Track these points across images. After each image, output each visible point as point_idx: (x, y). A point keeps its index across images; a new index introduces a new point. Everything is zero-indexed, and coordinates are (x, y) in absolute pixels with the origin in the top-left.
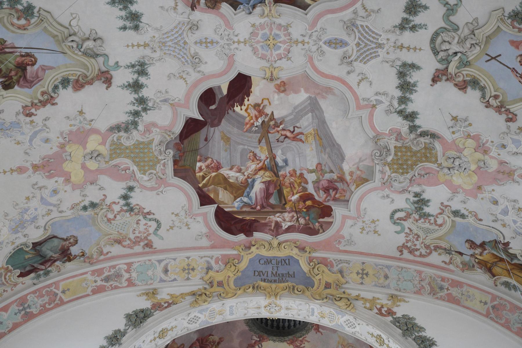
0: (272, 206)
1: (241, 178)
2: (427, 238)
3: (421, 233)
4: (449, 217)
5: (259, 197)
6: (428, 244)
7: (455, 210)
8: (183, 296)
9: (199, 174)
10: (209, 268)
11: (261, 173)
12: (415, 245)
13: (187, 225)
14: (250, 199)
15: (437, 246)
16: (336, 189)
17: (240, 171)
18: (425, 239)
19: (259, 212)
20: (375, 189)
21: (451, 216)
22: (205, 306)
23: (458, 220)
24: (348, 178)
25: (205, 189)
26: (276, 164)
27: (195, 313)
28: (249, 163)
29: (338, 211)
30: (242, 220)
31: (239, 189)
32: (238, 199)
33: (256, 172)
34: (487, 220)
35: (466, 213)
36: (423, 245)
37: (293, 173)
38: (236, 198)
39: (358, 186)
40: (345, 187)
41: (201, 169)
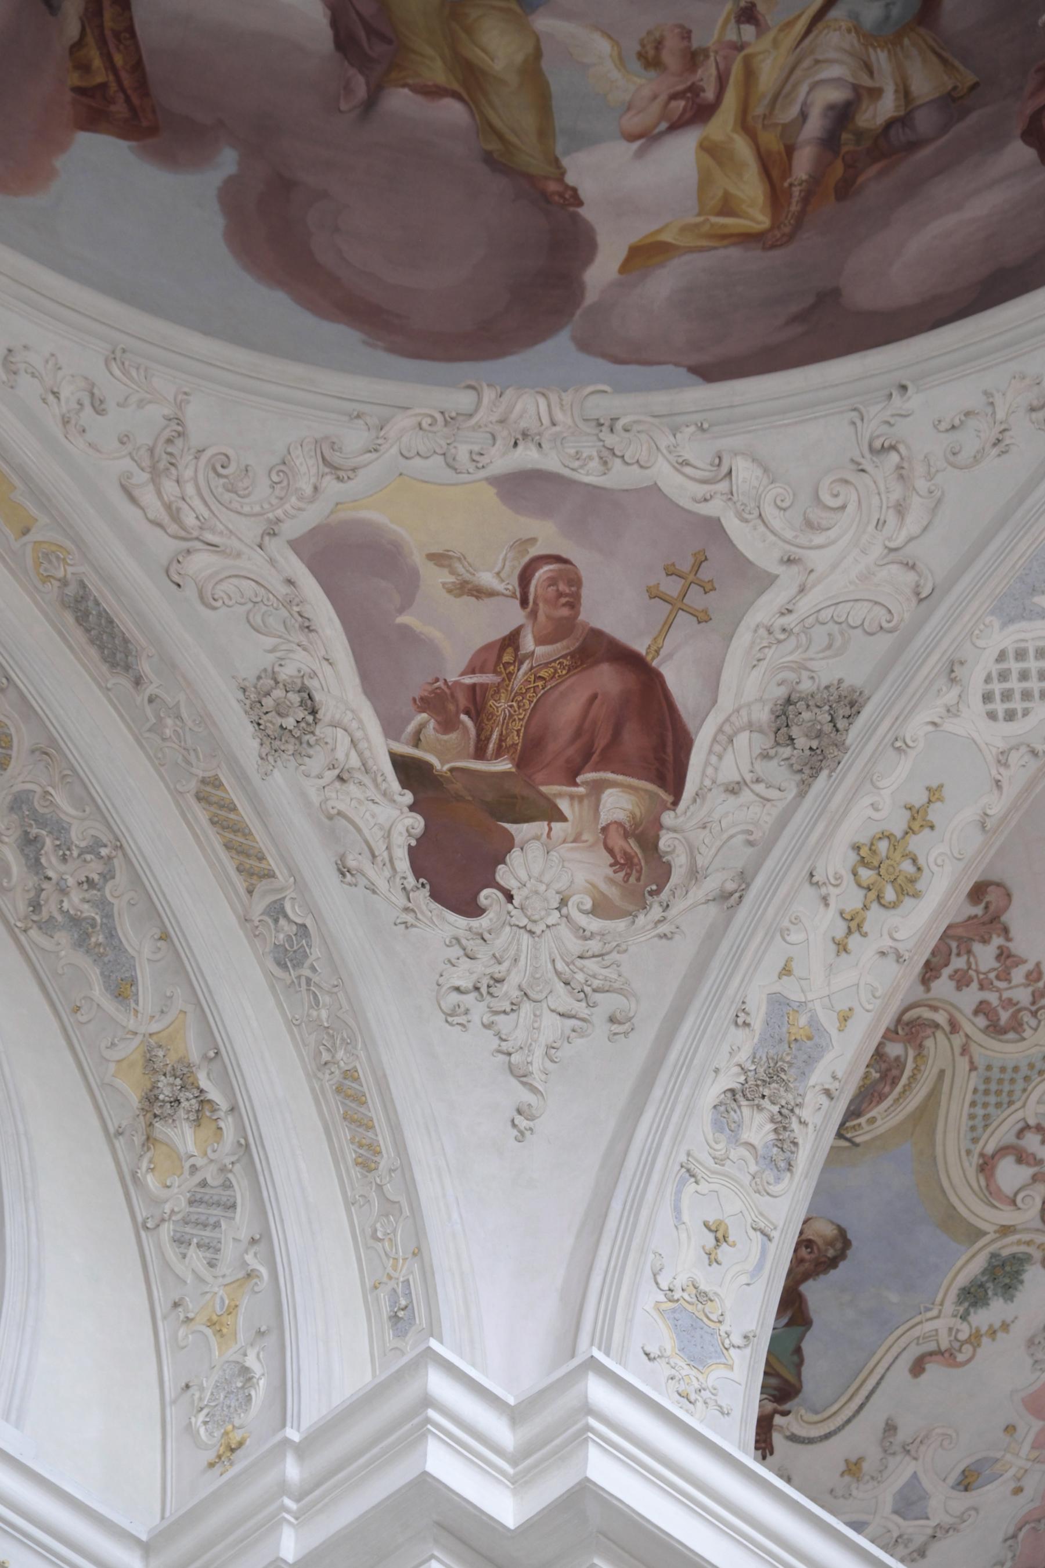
2: (963, 1064)
3: (1006, 1052)
4: (1005, 1230)
6: (929, 1043)
7: (1026, 1277)
12: (961, 981)
15: (894, 1082)
18: (965, 1050)
21: (1008, 1247)
23: (971, 1267)
34: (899, 1396)
35: (982, 1318)
36: (941, 1018)
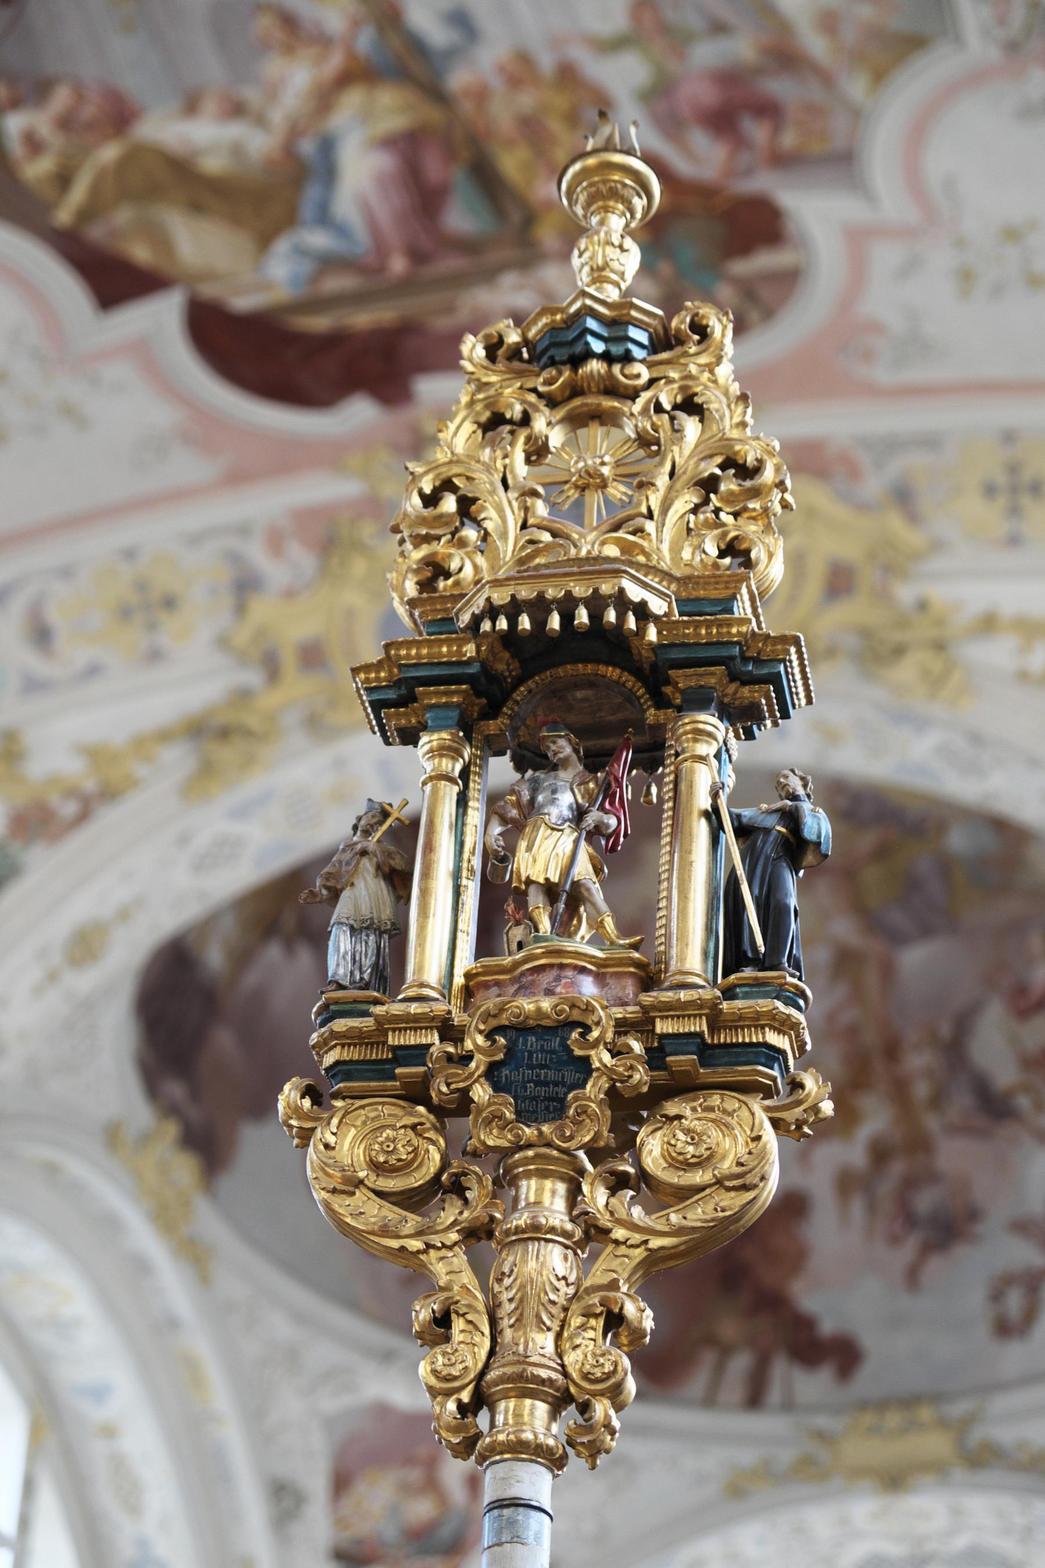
0: (467, 246)
1: (259, 143)
5: (384, 215)
8: (145, 744)
9: (37, 170)
10: (245, 586)
11: (353, 99)
13: (70, 412)
14: (341, 230)
16: (769, 110)
17: (236, 110)
19: (406, 286)
20: (975, 79)
22: (254, 785)
24: (816, 45)
25: (96, 233)
26: (417, 46)
27: (211, 821)
28: (274, 66)
29: (814, 211)
30: (335, 340)
31: (273, 196)
32: (282, 246)
33: (325, 98)
37: (521, 70)
38: (264, 241)
39: (879, 76)
40: (815, 92)
41: (34, 145)
